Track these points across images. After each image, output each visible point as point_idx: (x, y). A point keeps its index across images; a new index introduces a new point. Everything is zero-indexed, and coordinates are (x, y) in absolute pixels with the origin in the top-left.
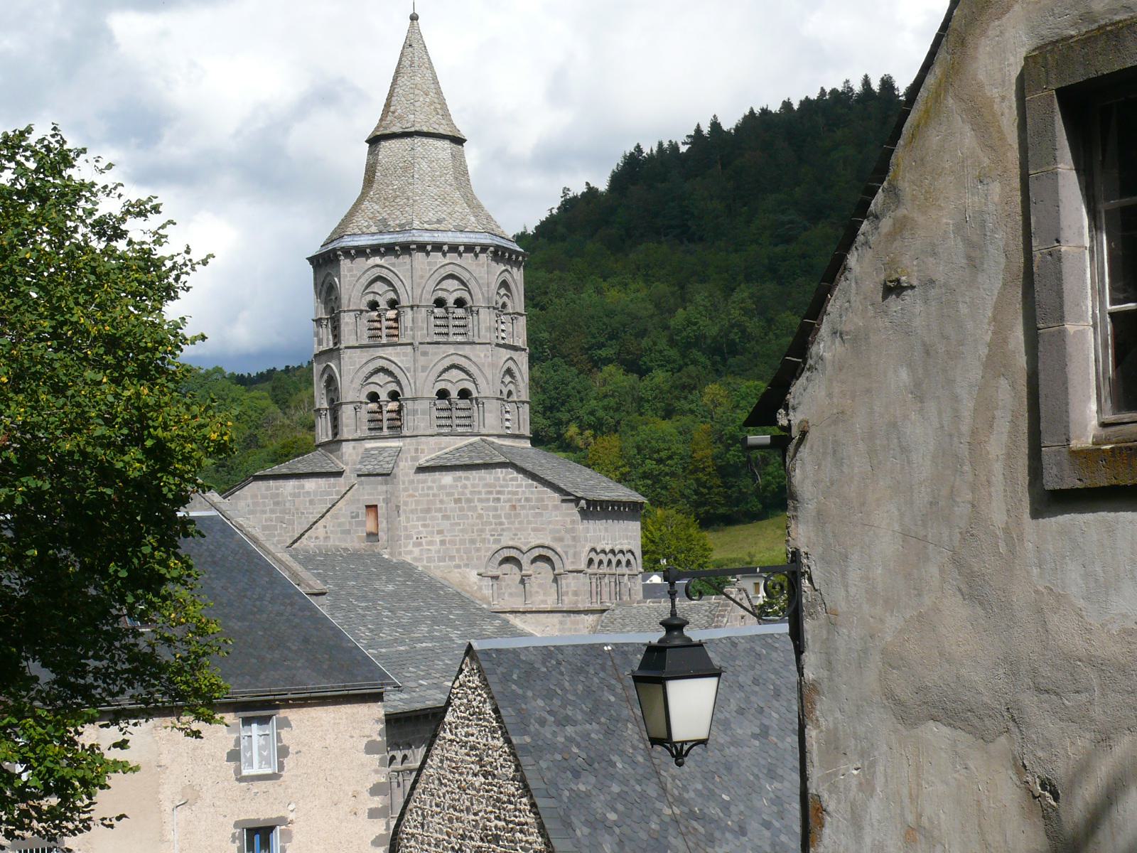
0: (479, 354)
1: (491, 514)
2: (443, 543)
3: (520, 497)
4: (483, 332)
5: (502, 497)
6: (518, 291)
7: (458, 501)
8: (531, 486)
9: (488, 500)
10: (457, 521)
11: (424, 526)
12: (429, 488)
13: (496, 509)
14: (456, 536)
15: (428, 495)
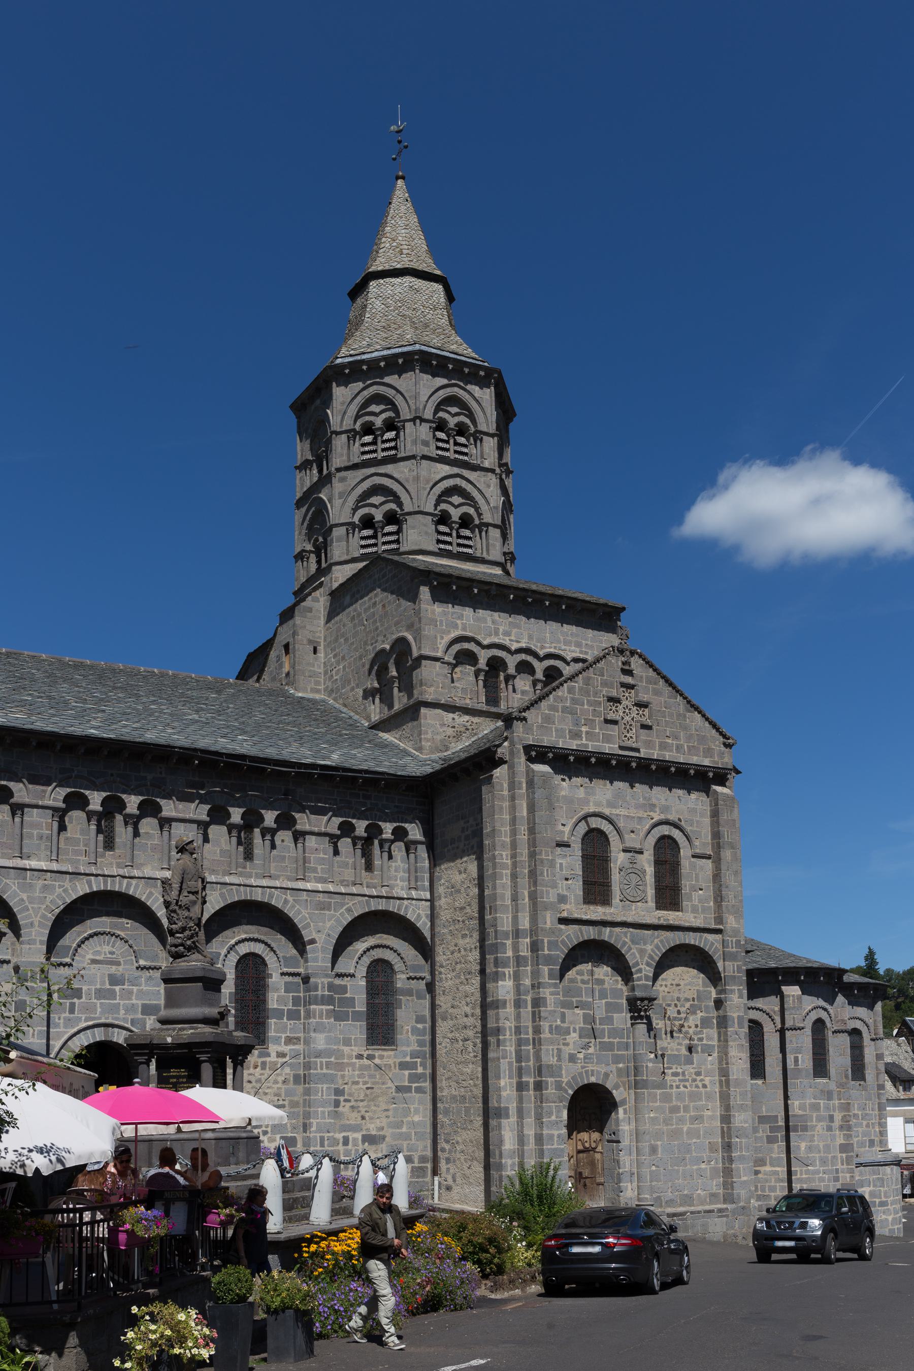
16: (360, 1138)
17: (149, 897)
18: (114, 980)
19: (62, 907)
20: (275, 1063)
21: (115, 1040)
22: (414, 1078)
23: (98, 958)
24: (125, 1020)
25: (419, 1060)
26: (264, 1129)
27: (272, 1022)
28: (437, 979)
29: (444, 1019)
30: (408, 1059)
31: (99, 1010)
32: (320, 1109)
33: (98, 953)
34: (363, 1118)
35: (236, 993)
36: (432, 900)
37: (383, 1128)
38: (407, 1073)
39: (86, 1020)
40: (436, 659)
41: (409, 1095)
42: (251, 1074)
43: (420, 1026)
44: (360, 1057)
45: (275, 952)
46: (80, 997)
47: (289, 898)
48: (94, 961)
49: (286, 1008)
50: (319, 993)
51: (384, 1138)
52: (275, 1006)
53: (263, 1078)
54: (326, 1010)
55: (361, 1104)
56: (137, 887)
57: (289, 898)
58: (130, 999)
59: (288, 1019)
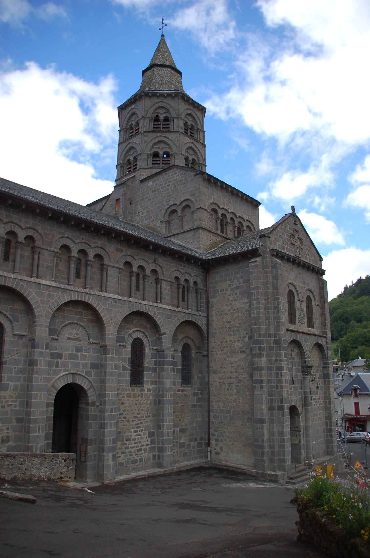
0: (173, 136)
1: (166, 192)
2: (148, 212)
3: (177, 181)
4: (175, 128)
5: (170, 183)
6: (199, 120)
7: (154, 191)
8: (182, 174)
9: (165, 187)
10: (153, 200)
11: (141, 207)
12: (144, 189)
13: (168, 189)
14: (153, 207)
15: (143, 193)
16: (179, 430)
17: (98, 305)
18: (78, 349)
19: (57, 307)
20: (147, 394)
21: (77, 383)
22: (198, 400)
23: (71, 337)
24: (82, 371)
25: (200, 392)
26: (142, 428)
27: (146, 373)
28: (210, 353)
29: (215, 372)
30: (196, 391)
31: (70, 365)
32: (168, 418)
33: (70, 334)
34: (180, 420)
35: (131, 358)
36: (207, 317)
37: (186, 425)
38: (196, 398)
39: (64, 371)
40: (205, 210)
41: (196, 408)
42: (136, 400)
43: (200, 375)
44: (179, 390)
45: (147, 338)
46: (61, 358)
47: (156, 312)
48: (69, 338)
49: (151, 366)
50: (168, 359)
51: (187, 429)
52: (147, 366)
53: (142, 402)
54: (171, 368)
55: (179, 414)
56: (93, 299)
57: (156, 312)
58: (85, 360)
59: (152, 372)
